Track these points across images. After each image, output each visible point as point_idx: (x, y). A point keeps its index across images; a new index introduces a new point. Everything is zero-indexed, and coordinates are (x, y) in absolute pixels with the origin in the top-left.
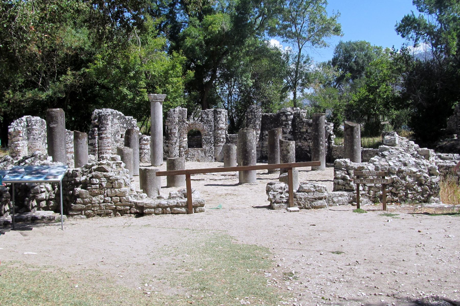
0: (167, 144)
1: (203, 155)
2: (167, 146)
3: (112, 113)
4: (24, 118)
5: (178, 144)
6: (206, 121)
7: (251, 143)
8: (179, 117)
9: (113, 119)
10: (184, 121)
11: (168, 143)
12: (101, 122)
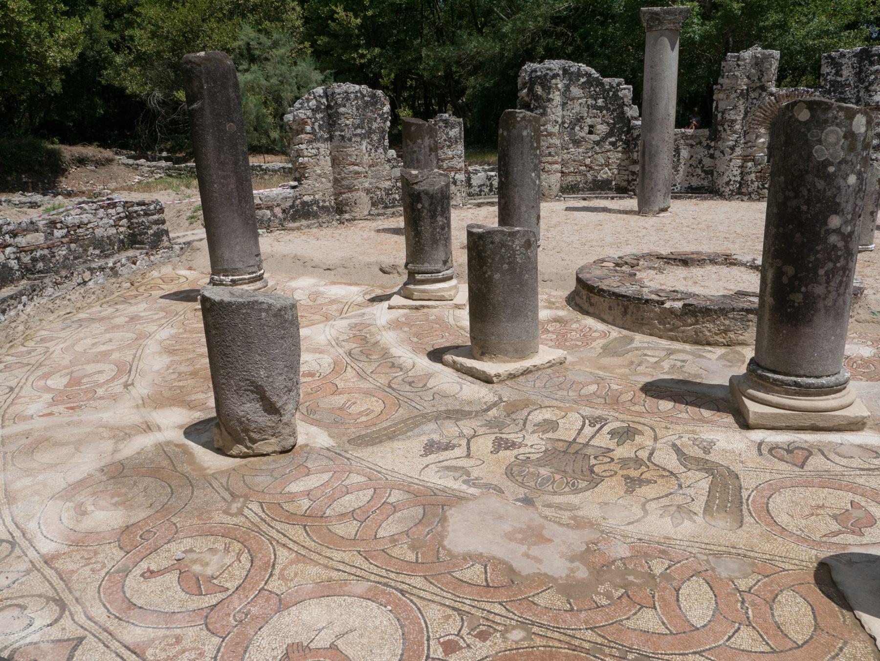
0: (712, 151)
2: (712, 156)
3: (565, 71)
5: (738, 151)
6: (832, 86)
7: (829, 179)
8: (748, 77)
9: (567, 88)
10: (763, 88)
11: (715, 148)
12: (533, 95)
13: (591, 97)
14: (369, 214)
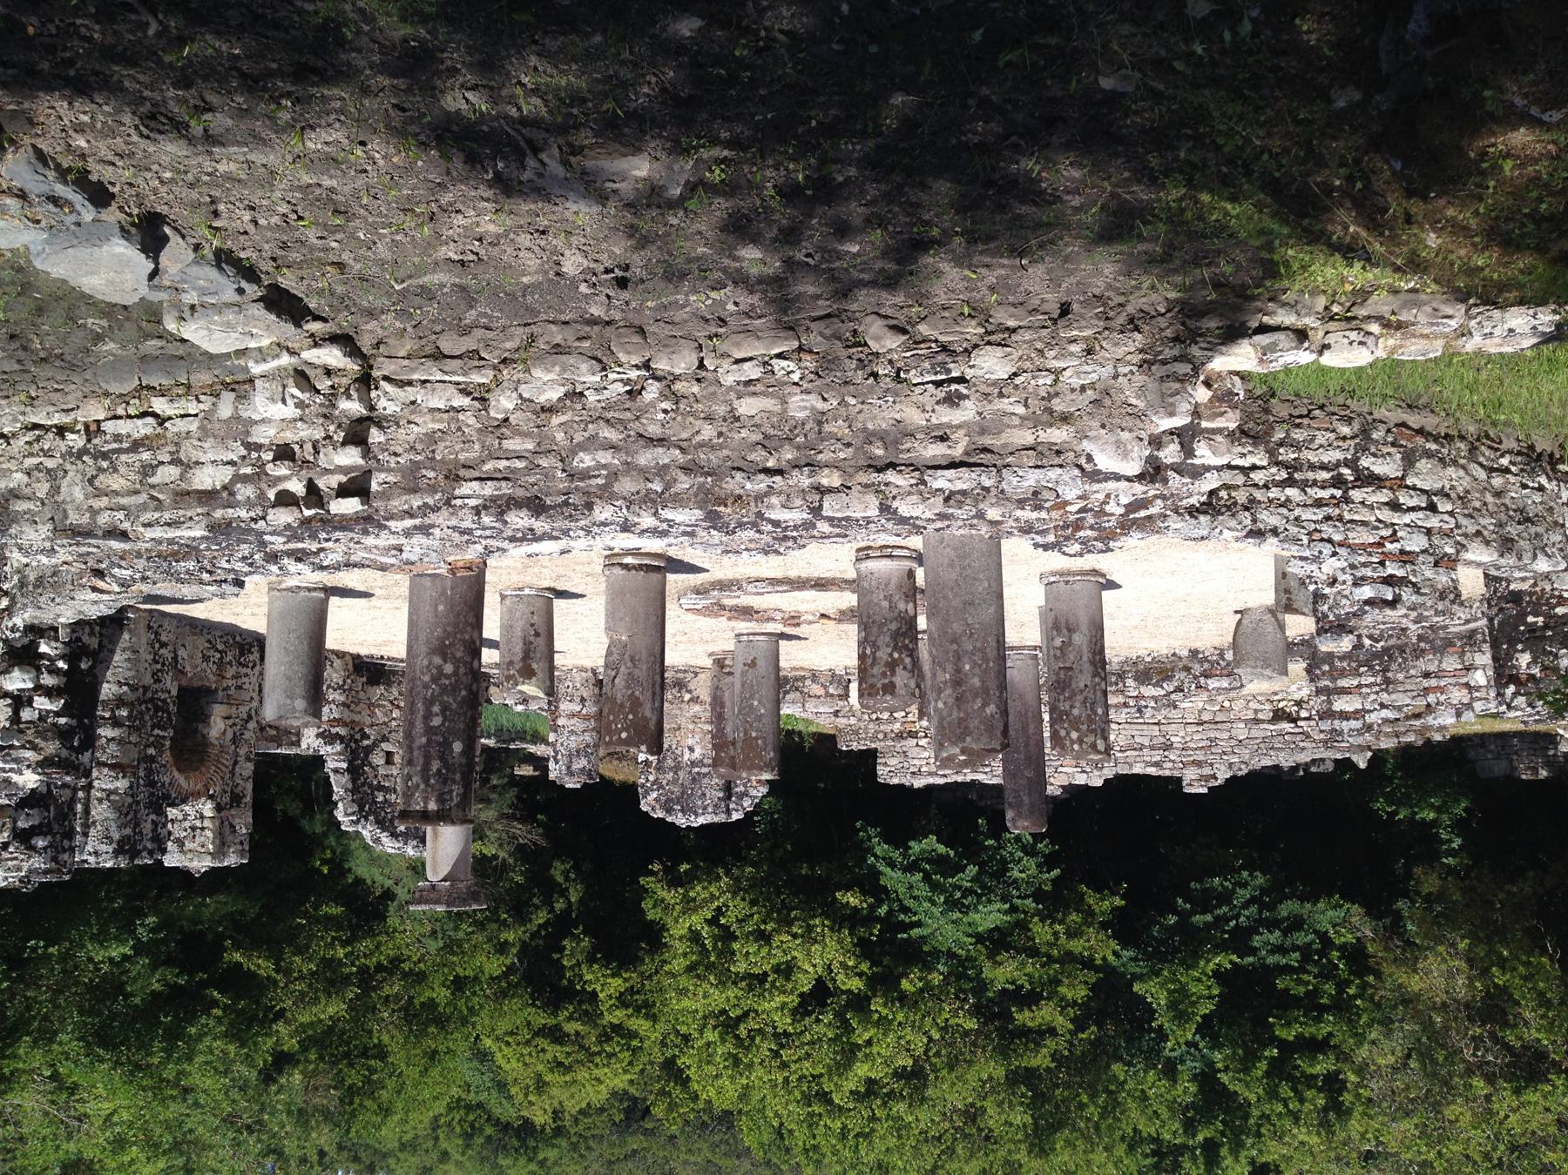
1: (182, 653)
4: (736, 816)
5: (244, 709)
13: (391, 805)
14: (696, 674)
